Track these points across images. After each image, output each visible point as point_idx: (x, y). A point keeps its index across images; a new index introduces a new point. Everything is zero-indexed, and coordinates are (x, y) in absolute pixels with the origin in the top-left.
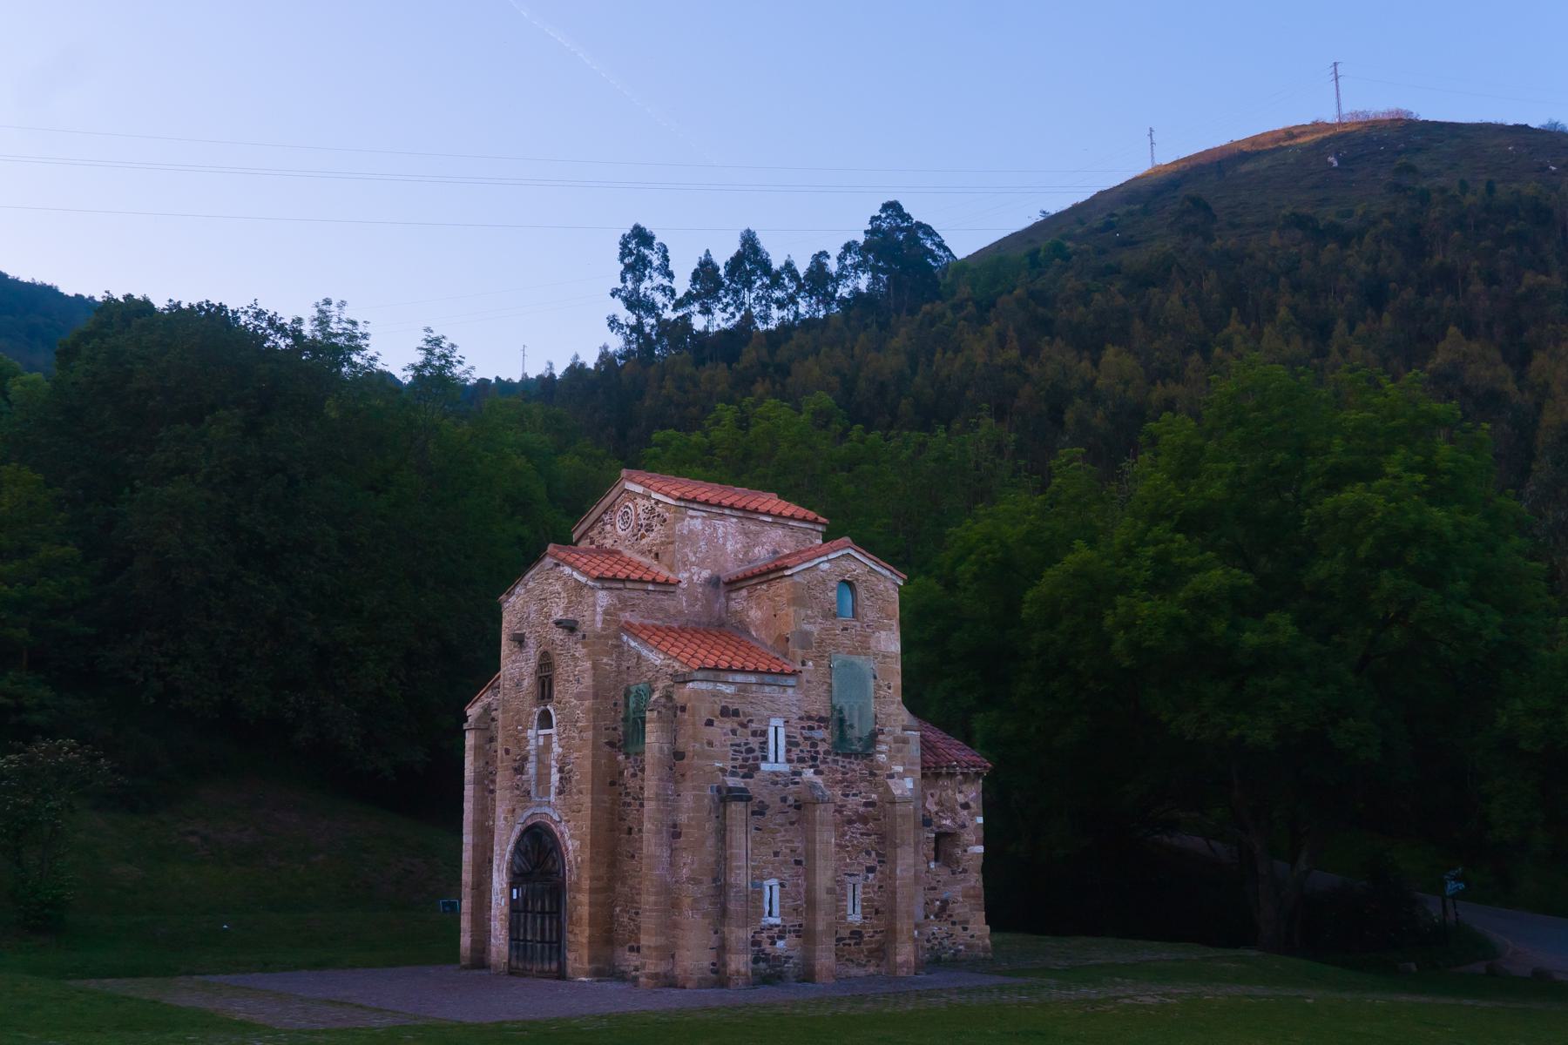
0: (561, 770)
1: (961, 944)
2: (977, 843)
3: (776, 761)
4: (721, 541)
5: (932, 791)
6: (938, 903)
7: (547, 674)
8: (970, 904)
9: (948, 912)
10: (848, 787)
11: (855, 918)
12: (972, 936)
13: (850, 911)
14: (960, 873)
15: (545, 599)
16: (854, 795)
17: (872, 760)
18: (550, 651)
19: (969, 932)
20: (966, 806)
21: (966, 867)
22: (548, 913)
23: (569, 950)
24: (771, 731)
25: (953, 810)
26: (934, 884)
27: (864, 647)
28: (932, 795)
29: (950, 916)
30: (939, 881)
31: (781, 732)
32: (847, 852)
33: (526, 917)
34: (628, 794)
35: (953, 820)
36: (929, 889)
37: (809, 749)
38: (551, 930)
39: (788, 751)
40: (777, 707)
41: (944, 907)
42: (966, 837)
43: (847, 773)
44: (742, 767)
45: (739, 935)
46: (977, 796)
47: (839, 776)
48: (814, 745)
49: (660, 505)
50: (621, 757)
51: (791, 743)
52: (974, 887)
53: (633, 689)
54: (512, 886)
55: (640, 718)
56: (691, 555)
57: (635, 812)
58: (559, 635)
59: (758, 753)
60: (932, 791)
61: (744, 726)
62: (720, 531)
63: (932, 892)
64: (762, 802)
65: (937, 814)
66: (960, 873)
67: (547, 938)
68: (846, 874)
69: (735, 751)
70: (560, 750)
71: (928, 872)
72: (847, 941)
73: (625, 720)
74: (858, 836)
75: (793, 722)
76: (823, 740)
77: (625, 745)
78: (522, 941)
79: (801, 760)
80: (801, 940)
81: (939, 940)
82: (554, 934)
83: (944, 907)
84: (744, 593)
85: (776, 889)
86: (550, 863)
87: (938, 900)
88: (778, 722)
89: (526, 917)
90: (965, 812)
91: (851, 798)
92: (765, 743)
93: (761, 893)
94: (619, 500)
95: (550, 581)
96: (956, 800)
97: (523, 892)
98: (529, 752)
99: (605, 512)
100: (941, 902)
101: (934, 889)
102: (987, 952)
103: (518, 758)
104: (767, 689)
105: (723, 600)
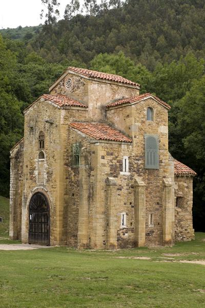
0: (48, 173)
3: (125, 171)
4: (104, 92)
20: (187, 187)
23: (52, 236)
27: (156, 131)
31: (127, 161)
33: (35, 224)
34: (72, 182)
45: (113, 232)
50: (70, 169)
53: (74, 145)
54: (30, 213)
56: (93, 97)
58: (47, 125)
62: (104, 89)
67: (43, 232)
73: (71, 156)
77: (71, 165)
79: (134, 171)
80: (133, 234)
82: (46, 231)
84: (113, 111)
85: (125, 216)
99: (61, 81)
105: (104, 113)
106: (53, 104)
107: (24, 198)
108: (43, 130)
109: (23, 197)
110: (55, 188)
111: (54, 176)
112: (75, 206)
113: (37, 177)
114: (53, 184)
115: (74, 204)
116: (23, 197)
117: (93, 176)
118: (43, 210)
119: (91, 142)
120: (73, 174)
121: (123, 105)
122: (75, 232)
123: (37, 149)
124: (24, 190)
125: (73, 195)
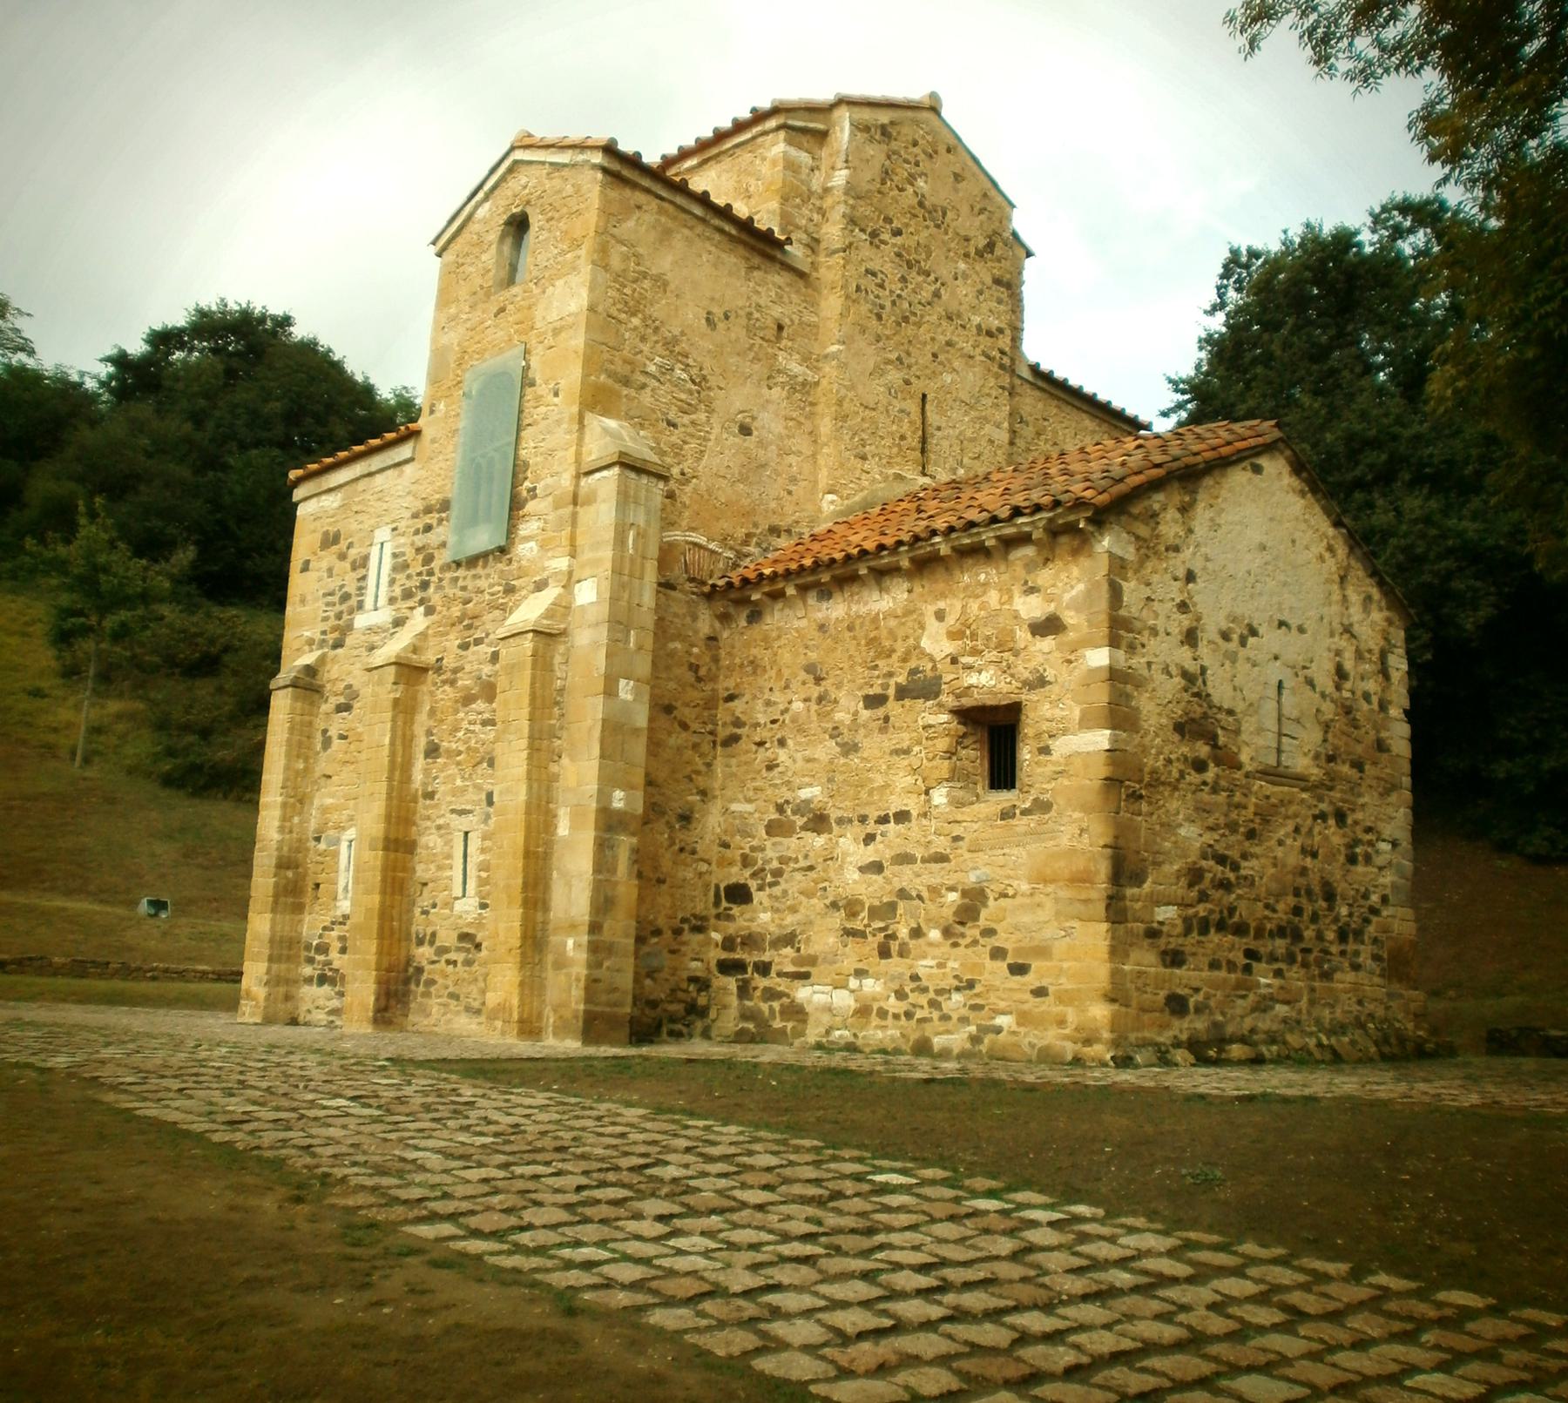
1: (1003, 1013)
2: (1086, 723)
5: (941, 604)
6: (953, 897)
8: (1057, 900)
9: (983, 922)
10: (469, 627)
11: (467, 907)
12: (1040, 992)
13: (458, 892)
14: (1025, 812)
16: (478, 642)
17: (510, 561)
19: (1031, 980)
20: (1049, 626)
21: (1045, 797)
24: (375, 551)
25: (1005, 645)
26: (941, 845)
28: (940, 616)
29: (989, 932)
30: (957, 839)
32: (458, 764)
35: (1007, 669)
36: (924, 861)
37: (420, 569)
39: (392, 582)
40: (385, 506)
41: (968, 911)
42: (1046, 710)
43: (469, 601)
44: (334, 629)
46: (1088, 594)
47: (456, 611)
48: (429, 559)
51: (400, 567)
52: (1072, 851)
59: (353, 602)
60: (941, 604)
61: (342, 557)
63: (935, 867)
64: (349, 687)
65: (954, 661)
66: (1025, 812)
68: (453, 811)
69: (328, 604)
71: (925, 815)
72: (452, 956)
74: (477, 728)
75: (402, 525)
76: (444, 545)
79: (407, 595)
81: (932, 995)
83: (972, 903)
87: (952, 889)
88: (383, 534)
90: (1047, 643)
91: (473, 649)
92: (364, 578)
93: (336, 854)
96: (1016, 616)
100: (965, 894)
101: (941, 858)
102: (1088, 1042)
104: (379, 479)
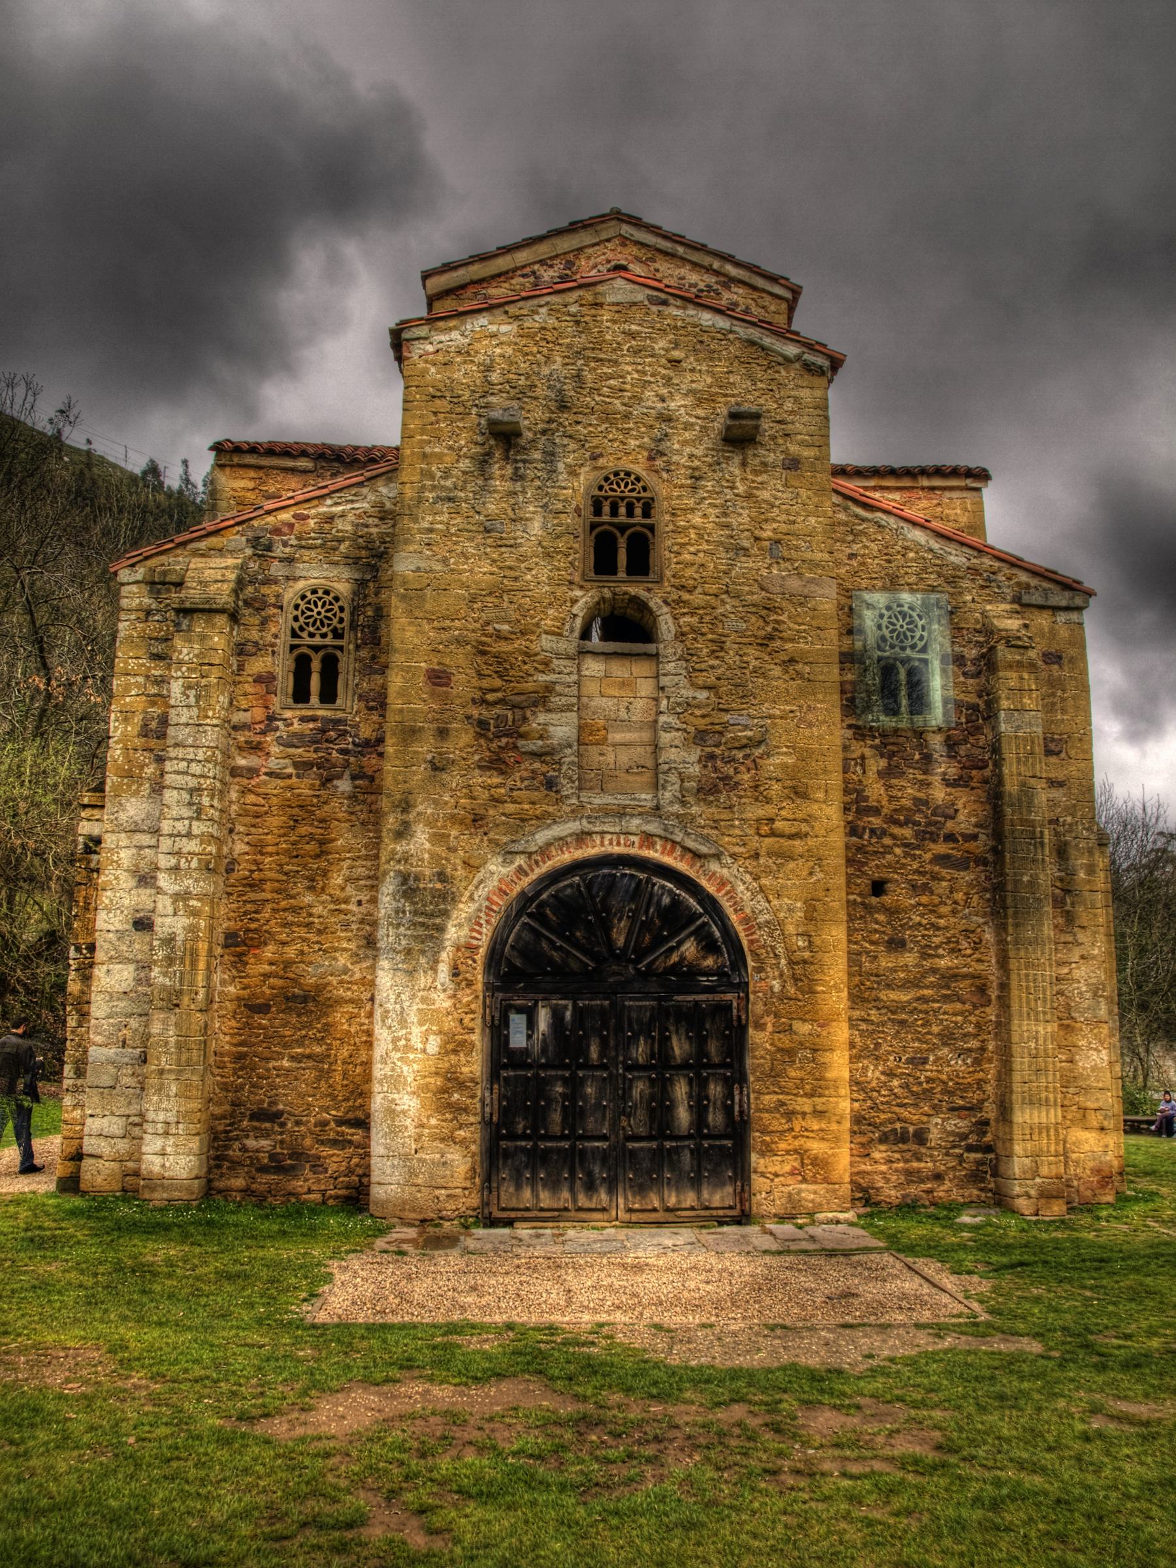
0: (700, 737)
7: (622, 519)
15: (616, 363)
18: (643, 474)
22: (684, 1066)
23: (768, 1150)
34: (876, 811)
38: (699, 1109)
49: (734, 289)
55: (904, 662)
57: (898, 851)
70: (702, 695)
78: (563, 1137)
82: (715, 1118)
86: (689, 948)
89: (574, 1085)
94: (590, 251)
95: (634, 327)
97: (557, 1016)
98: (549, 688)
103: (490, 697)
106: (754, 333)
107: (409, 887)
108: (639, 469)
109: (388, 888)
110: (792, 837)
111: (778, 761)
112: (910, 958)
113: (569, 756)
114: (769, 810)
115: (896, 945)
116: (388, 888)
117: (1061, 784)
118: (687, 976)
119: (1036, 598)
120: (876, 764)
121: (925, 482)
122: (905, 1113)
123: (577, 578)
124: (403, 832)
125: (878, 888)
